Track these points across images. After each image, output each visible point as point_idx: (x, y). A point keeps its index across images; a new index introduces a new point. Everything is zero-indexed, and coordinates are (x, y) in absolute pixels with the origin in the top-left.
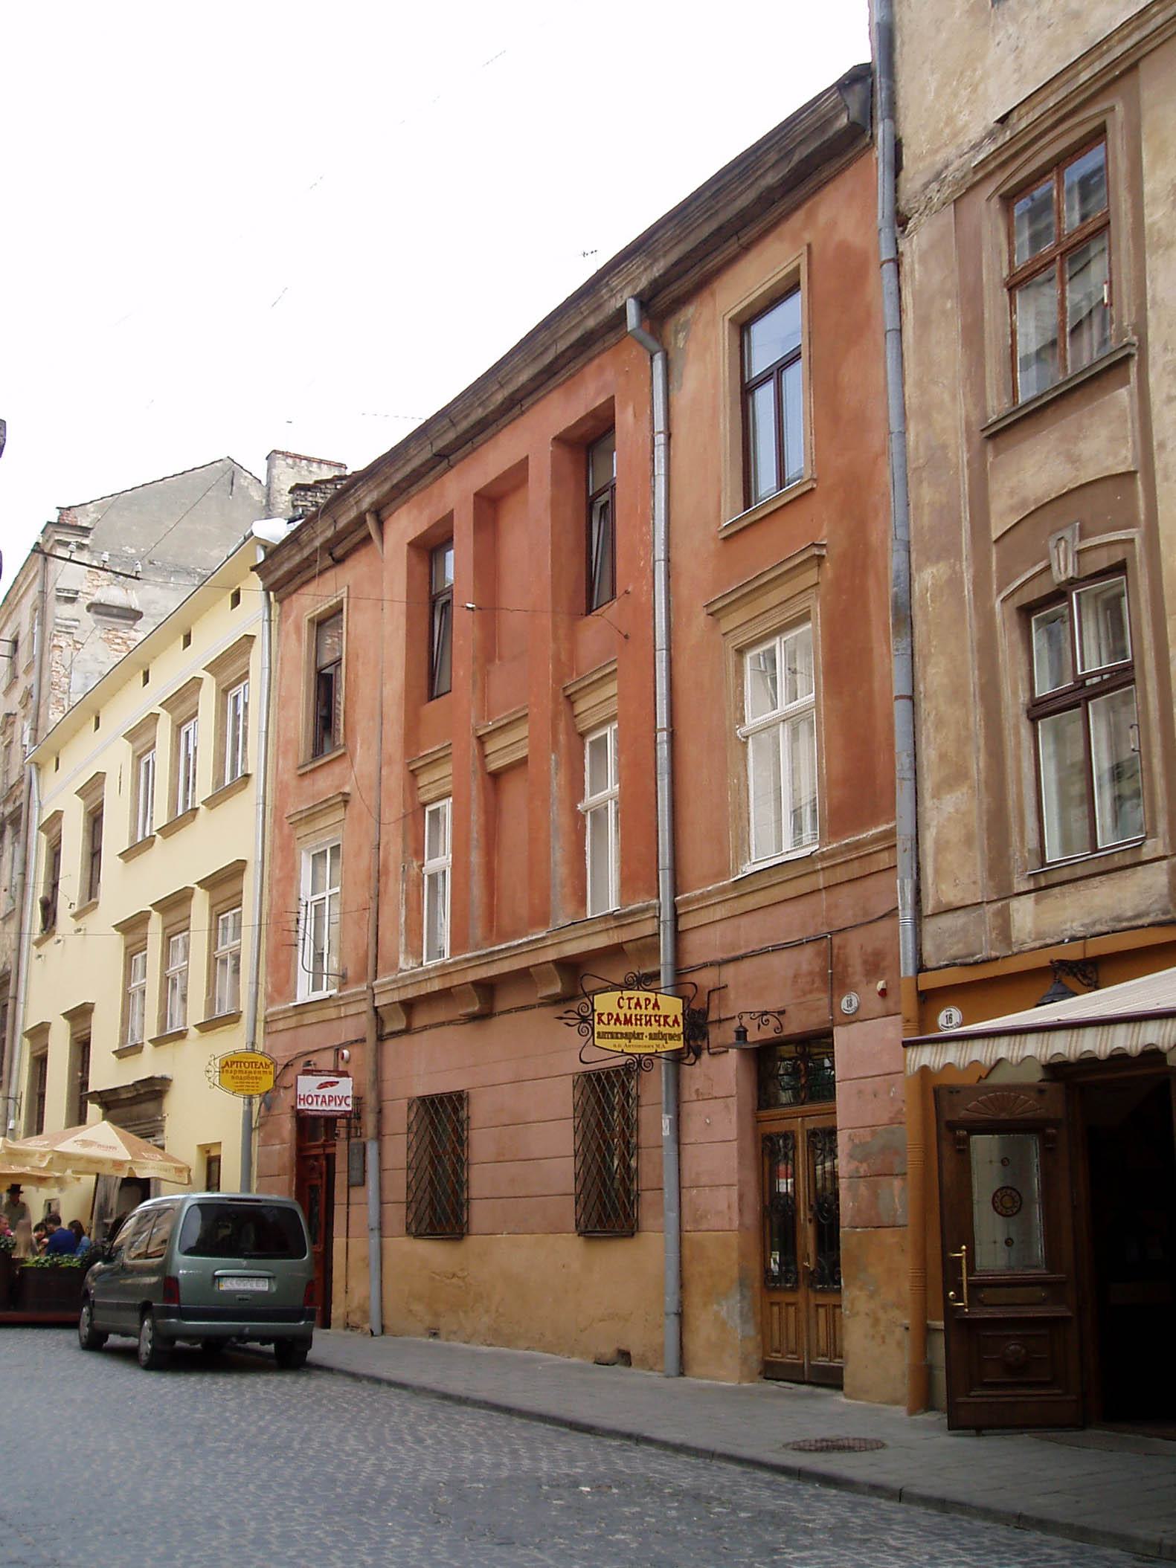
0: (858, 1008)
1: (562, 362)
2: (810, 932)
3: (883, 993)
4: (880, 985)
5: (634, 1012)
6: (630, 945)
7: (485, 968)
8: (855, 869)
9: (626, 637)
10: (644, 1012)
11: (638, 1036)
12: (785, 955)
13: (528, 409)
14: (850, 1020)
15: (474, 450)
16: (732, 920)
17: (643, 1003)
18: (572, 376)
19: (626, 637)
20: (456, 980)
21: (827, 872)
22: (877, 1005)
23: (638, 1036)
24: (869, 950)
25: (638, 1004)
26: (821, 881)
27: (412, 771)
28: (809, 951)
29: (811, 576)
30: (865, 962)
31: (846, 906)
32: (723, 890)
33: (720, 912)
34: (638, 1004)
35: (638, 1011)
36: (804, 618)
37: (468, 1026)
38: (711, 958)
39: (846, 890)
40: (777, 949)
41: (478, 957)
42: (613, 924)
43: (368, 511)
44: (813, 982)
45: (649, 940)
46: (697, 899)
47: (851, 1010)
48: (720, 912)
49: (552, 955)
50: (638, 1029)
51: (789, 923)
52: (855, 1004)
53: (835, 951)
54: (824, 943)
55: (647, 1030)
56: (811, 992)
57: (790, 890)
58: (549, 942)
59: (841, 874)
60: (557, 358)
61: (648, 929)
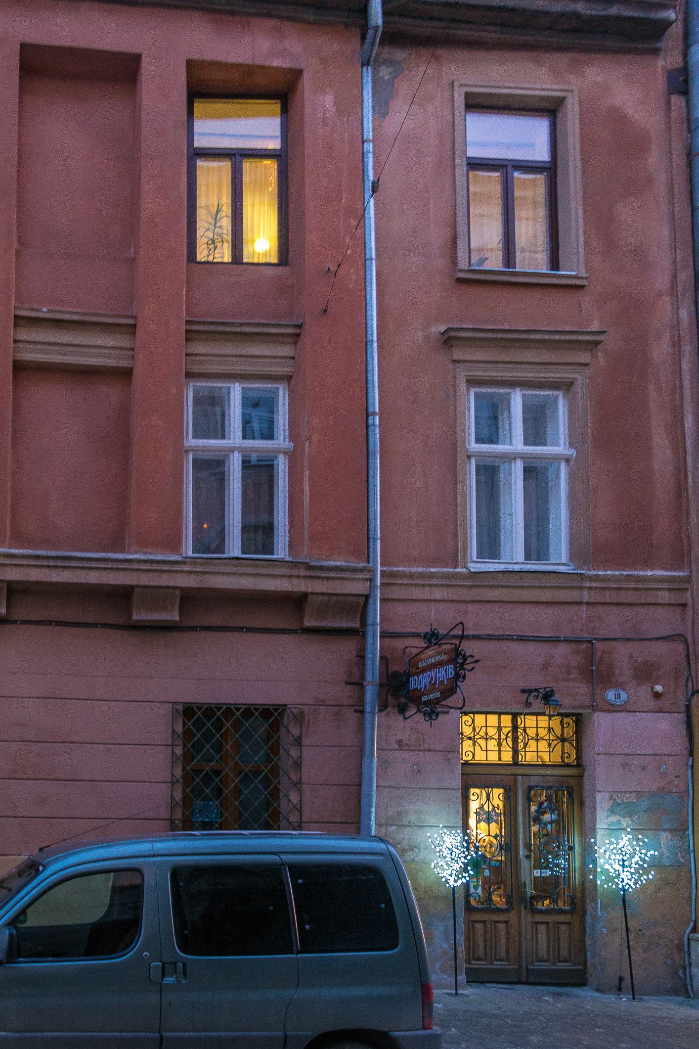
0: (626, 702)
2: (567, 633)
3: (657, 695)
4: (659, 688)
6: (320, 598)
7: (47, 571)
8: (630, 597)
12: (532, 647)
14: (612, 709)
16: (454, 604)
21: (593, 592)
22: (651, 703)
24: (640, 660)
26: (586, 596)
28: (563, 649)
29: (583, 357)
30: (636, 669)
31: (613, 622)
32: (455, 576)
36: (567, 386)
39: (613, 610)
40: (521, 639)
41: (37, 557)
42: (303, 573)
44: (569, 674)
46: (411, 576)
47: (619, 702)
48: (438, 594)
49: (184, 581)
51: (544, 620)
52: (624, 696)
53: (599, 654)
54: (585, 645)
56: (567, 680)
57: (546, 596)
58: (186, 568)
59: (607, 597)
61: (358, 588)
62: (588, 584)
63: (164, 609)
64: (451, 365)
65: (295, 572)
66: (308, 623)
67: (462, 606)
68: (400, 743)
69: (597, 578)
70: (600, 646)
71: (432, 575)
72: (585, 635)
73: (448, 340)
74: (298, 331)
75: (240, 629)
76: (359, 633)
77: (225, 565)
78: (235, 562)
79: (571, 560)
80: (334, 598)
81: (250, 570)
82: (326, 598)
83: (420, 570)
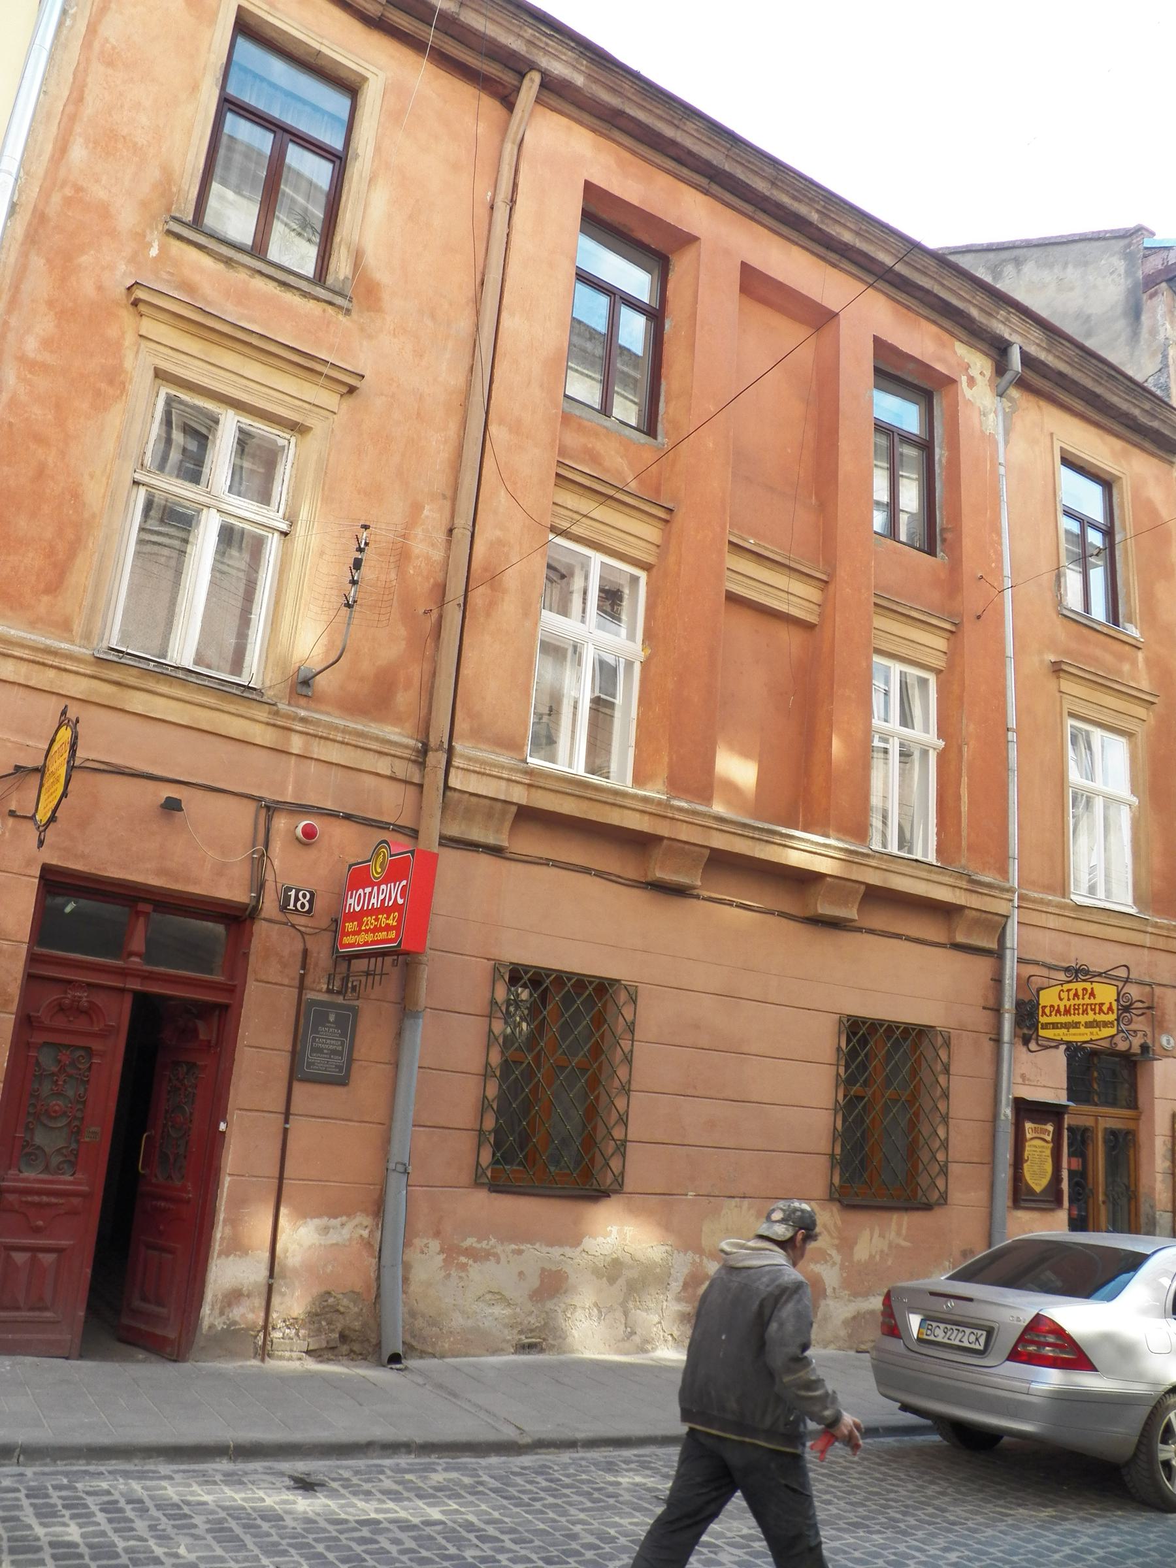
1: (920, 294)
5: (1072, 1002)
6: (974, 912)
7: (750, 842)
9: (979, 617)
10: (1081, 1001)
11: (1076, 1025)
13: (841, 269)
15: (752, 218)
17: (1080, 993)
18: (908, 308)
19: (979, 617)
20: (685, 834)
23: (1076, 1025)
25: (1076, 995)
26: (1147, 940)
27: (557, 474)
33: (1053, 922)
34: (1076, 995)
35: (1076, 1002)
37: (636, 893)
38: (1040, 958)
41: (744, 825)
42: (964, 885)
43: (544, 74)
45: (997, 918)
48: (1053, 922)
50: (1076, 1018)
55: (1083, 1019)
58: (873, 863)
60: (921, 288)
62: (1150, 929)
63: (845, 904)
64: (1058, 695)
65: (959, 883)
66: (960, 939)
67: (1067, 936)
68: (1023, 1076)
69: (1156, 925)
70: (1158, 990)
71: (1049, 903)
72: (1148, 980)
73: (1057, 669)
74: (953, 629)
75: (898, 936)
76: (998, 955)
77: (908, 866)
78: (914, 864)
79: (1135, 903)
80: (984, 915)
81: (924, 875)
82: (978, 914)
83: (1041, 896)
